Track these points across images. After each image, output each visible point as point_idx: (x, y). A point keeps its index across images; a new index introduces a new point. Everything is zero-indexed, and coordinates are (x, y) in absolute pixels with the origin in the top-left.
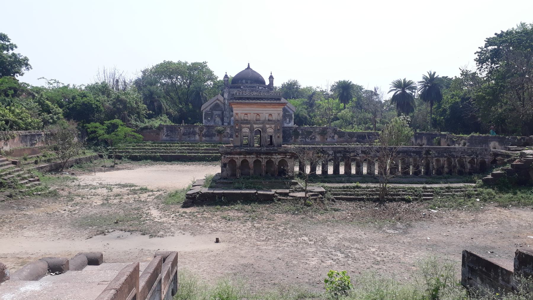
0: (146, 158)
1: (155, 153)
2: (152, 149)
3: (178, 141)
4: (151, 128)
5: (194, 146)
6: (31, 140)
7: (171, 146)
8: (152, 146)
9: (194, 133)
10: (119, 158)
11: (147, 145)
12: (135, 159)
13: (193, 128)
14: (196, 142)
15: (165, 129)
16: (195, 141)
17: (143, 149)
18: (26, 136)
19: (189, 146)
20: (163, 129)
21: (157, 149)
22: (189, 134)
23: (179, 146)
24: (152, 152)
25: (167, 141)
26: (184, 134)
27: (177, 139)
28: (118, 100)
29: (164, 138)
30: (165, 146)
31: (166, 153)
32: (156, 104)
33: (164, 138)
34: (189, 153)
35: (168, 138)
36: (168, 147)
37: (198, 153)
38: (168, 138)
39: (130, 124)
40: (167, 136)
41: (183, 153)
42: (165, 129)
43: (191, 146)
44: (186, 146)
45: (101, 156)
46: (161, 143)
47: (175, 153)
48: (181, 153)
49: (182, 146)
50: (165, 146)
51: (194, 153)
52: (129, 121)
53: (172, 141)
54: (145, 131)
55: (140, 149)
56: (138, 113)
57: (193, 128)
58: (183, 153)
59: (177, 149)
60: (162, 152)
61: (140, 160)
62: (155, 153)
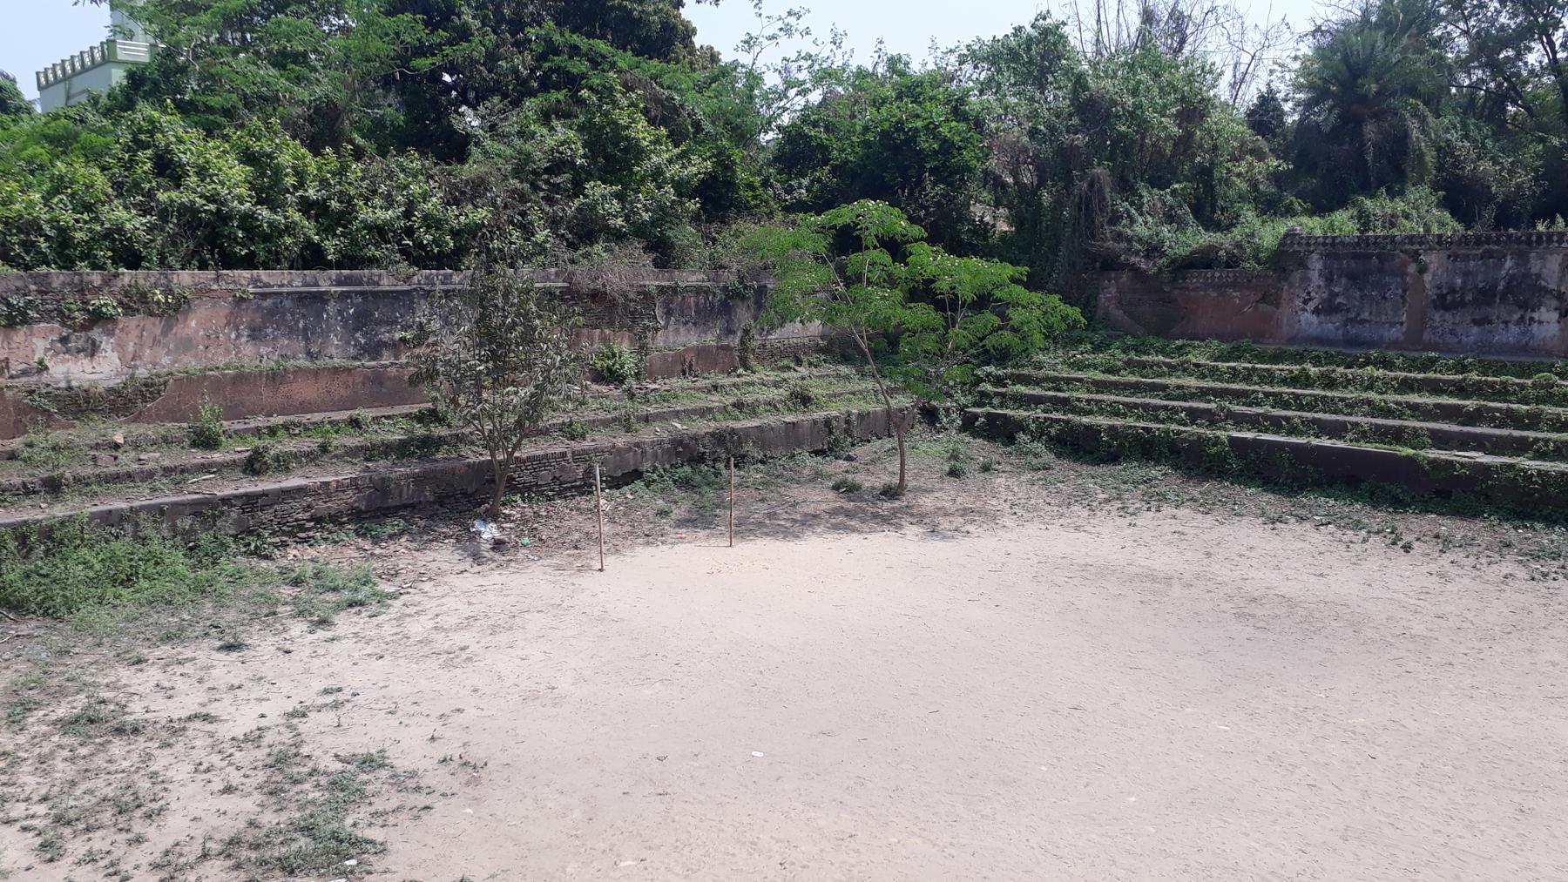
0: (1147, 449)
1: (1212, 419)
2: (1203, 394)
3: (1395, 344)
4: (1232, 262)
5: (1502, 393)
6: (361, 321)
7: (1331, 383)
8: (1214, 373)
9: (1525, 294)
10: (1001, 431)
11: (1184, 369)
12: (1081, 446)
13: (1522, 257)
14: (1528, 358)
15: (1316, 264)
16: (1524, 349)
17: (1154, 388)
18: (317, 299)
19: (1461, 390)
20: (1303, 264)
21: (1238, 395)
22: (1486, 296)
23: (1387, 385)
24: (1194, 415)
25: (1321, 341)
26: (1446, 301)
27: (1395, 333)
28: (1090, 109)
29: (1309, 321)
30: (1293, 381)
31: (1276, 424)
32: (1370, 130)
33: (1309, 321)
34: (1441, 440)
35: (1331, 326)
36: (1306, 381)
37: (1521, 447)
38: (1331, 326)
39: (1119, 237)
40: (1328, 308)
41: (1398, 436)
42: (1316, 264)
43: (1477, 390)
44: (1435, 388)
45: (930, 416)
46: (1275, 359)
47: (1336, 430)
48: (1381, 434)
49: (1406, 386)
50: (1293, 381)
51: (1480, 443)
52: (1115, 219)
53: (1350, 348)
54: (1195, 279)
55: (1136, 388)
56: (1204, 175)
57: (1522, 257)
58: (1398, 436)
59: (1365, 405)
60: (1254, 422)
61: (1114, 459)
62: (1212, 419)
